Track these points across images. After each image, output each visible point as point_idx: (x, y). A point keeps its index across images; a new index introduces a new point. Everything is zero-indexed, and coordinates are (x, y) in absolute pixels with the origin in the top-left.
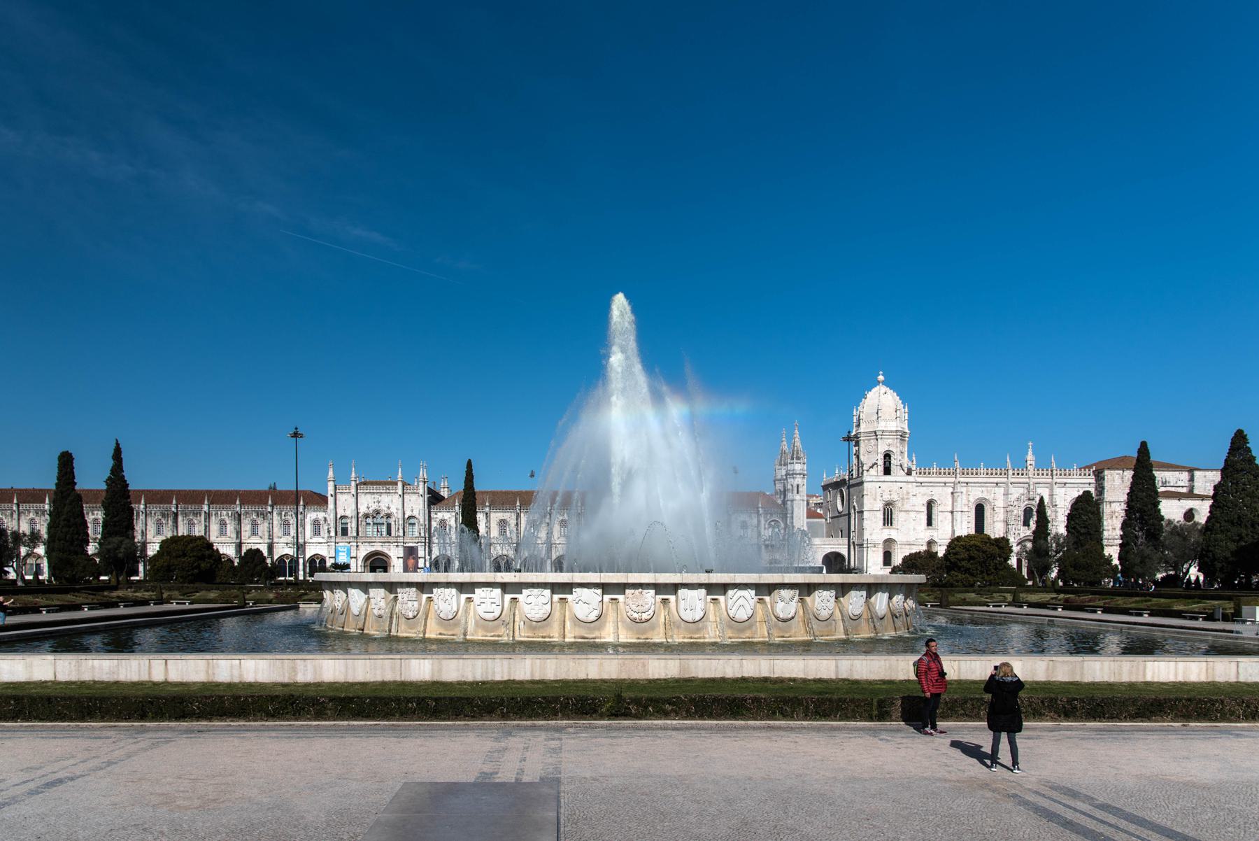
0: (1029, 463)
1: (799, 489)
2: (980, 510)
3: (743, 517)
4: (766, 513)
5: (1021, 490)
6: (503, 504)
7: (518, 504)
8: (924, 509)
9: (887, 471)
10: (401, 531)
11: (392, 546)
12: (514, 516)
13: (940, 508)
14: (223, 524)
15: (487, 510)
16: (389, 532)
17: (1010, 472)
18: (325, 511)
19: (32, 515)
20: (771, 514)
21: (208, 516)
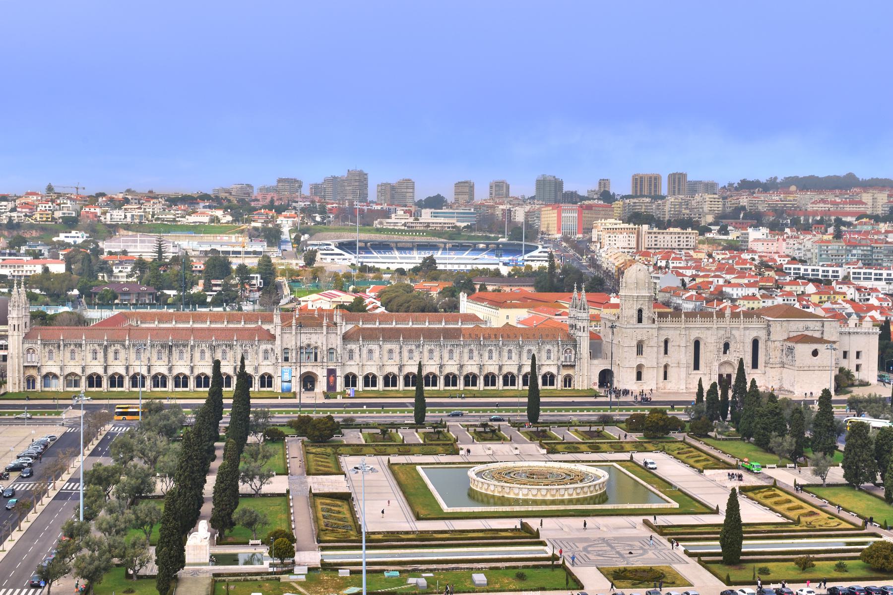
0: (726, 315)
1: (586, 329)
2: (697, 344)
3: (548, 347)
4: (563, 345)
5: (722, 332)
6: (390, 338)
7: (401, 339)
8: (663, 344)
9: (640, 320)
10: (325, 358)
11: (319, 369)
12: (398, 347)
13: (673, 344)
14: (203, 352)
15: (381, 343)
16: (316, 360)
17: (715, 321)
18: (273, 344)
19: (72, 347)
20: (567, 345)
21: (193, 347)
